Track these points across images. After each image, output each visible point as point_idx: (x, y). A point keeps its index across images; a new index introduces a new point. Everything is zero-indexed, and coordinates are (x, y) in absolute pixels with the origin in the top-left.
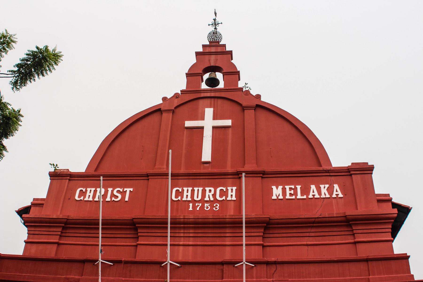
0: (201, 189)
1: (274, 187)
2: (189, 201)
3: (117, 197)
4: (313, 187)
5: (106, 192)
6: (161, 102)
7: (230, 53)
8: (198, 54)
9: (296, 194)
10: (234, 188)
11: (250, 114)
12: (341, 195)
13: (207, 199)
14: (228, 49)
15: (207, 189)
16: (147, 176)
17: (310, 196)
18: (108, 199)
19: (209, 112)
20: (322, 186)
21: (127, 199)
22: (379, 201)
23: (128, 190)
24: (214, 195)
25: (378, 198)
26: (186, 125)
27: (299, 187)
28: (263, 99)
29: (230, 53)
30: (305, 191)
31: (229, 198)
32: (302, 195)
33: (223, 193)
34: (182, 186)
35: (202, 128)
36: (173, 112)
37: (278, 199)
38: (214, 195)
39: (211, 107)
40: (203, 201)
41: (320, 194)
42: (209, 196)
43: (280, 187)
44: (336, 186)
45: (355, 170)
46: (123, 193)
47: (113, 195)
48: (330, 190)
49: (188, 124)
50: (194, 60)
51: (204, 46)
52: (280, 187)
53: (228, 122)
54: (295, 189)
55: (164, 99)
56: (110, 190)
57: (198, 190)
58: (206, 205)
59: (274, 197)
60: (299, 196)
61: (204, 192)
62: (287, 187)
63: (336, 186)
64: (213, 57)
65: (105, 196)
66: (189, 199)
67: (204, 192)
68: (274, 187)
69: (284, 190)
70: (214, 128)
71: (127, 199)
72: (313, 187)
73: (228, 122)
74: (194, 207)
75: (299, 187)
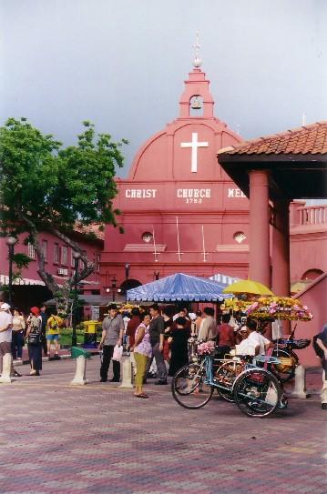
8: (186, 82)
11: (219, 136)
19: (195, 136)
23: (154, 191)
33: (204, 193)
35: (191, 148)
46: (152, 193)
47: (146, 194)
49: (184, 145)
53: (205, 144)
59: (229, 196)
64: (197, 86)
65: (142, 194)
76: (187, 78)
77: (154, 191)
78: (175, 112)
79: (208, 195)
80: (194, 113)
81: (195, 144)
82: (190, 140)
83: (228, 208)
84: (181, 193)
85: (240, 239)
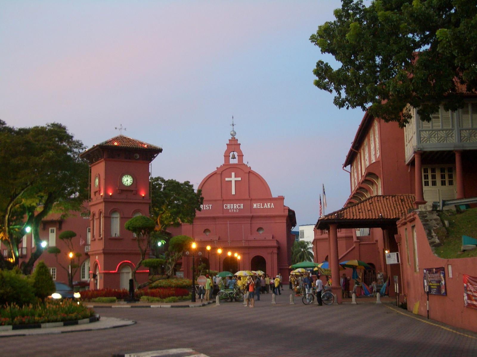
0: (232, 205)
1: (254, 204)
2: (229, 209)
3: (207, 208)
4: (266, 204)
5: (204, 206)
6: (216, 169)
7: (240, 144)
8: (227, 144)
9: (260, 206)
10: (242, 204)
12: (273, 207)
13: (234, 208)
14: (239, 142)
15: (234, 205)
16: (216, 200)
17: (265, 207)
18: (205, 209)
19: (233, 174)
20: (268, 204)
21: (210, 208)
22: (284, 209)
23: (210, 205)
24: (237, 207)
25: (285, 208)
26: (226, 180)
27: (261, 204)
28: (251, 169)
29: (240, 144)
30: (263, 205)
31: (241, 208)
32: (262, 207)
33: (239, 206)
34: (227, 204)
36: (221, 174)
37: (255, 208)
38: (237, 207)
39: (233, 172)
40: (233, 209)
41: (267, 206)
42: (235, 207)
43: (256, 204)
44: (272, 204)
45: (279, 199)
46: (209, 207)
47: (206, 207)
48: (270, 205)
49: (227, 179)
50: (225, 148)
51: (229, 140)
52: (256, 204)
53: (239, 179)
54: (260, 205)
55: (217, 168)
56: (205, 205)
57: (232, 205)
58: (234, 210)
59: (254, 207)
60: (261, 207)
61: (233, 205)
62: (258, 204)
63: (272, 204)
66: (229, 208)
67: (233, 205)
68: (254, 204)
69: (257, 205)
70: (235, 181)
71: (210, 208)
72: (266, 204)
73: (239, 179)
74: (231, 211)
75: (261, 204)
76: (228, 143)
77: (210, 205)
78: (221, 162)
79: (242, 207)
80: (232, 161)
81: (233, 179)
82: (231, 177)
83: (255, 214)
84: (226, 206)
85: (261, 232)
